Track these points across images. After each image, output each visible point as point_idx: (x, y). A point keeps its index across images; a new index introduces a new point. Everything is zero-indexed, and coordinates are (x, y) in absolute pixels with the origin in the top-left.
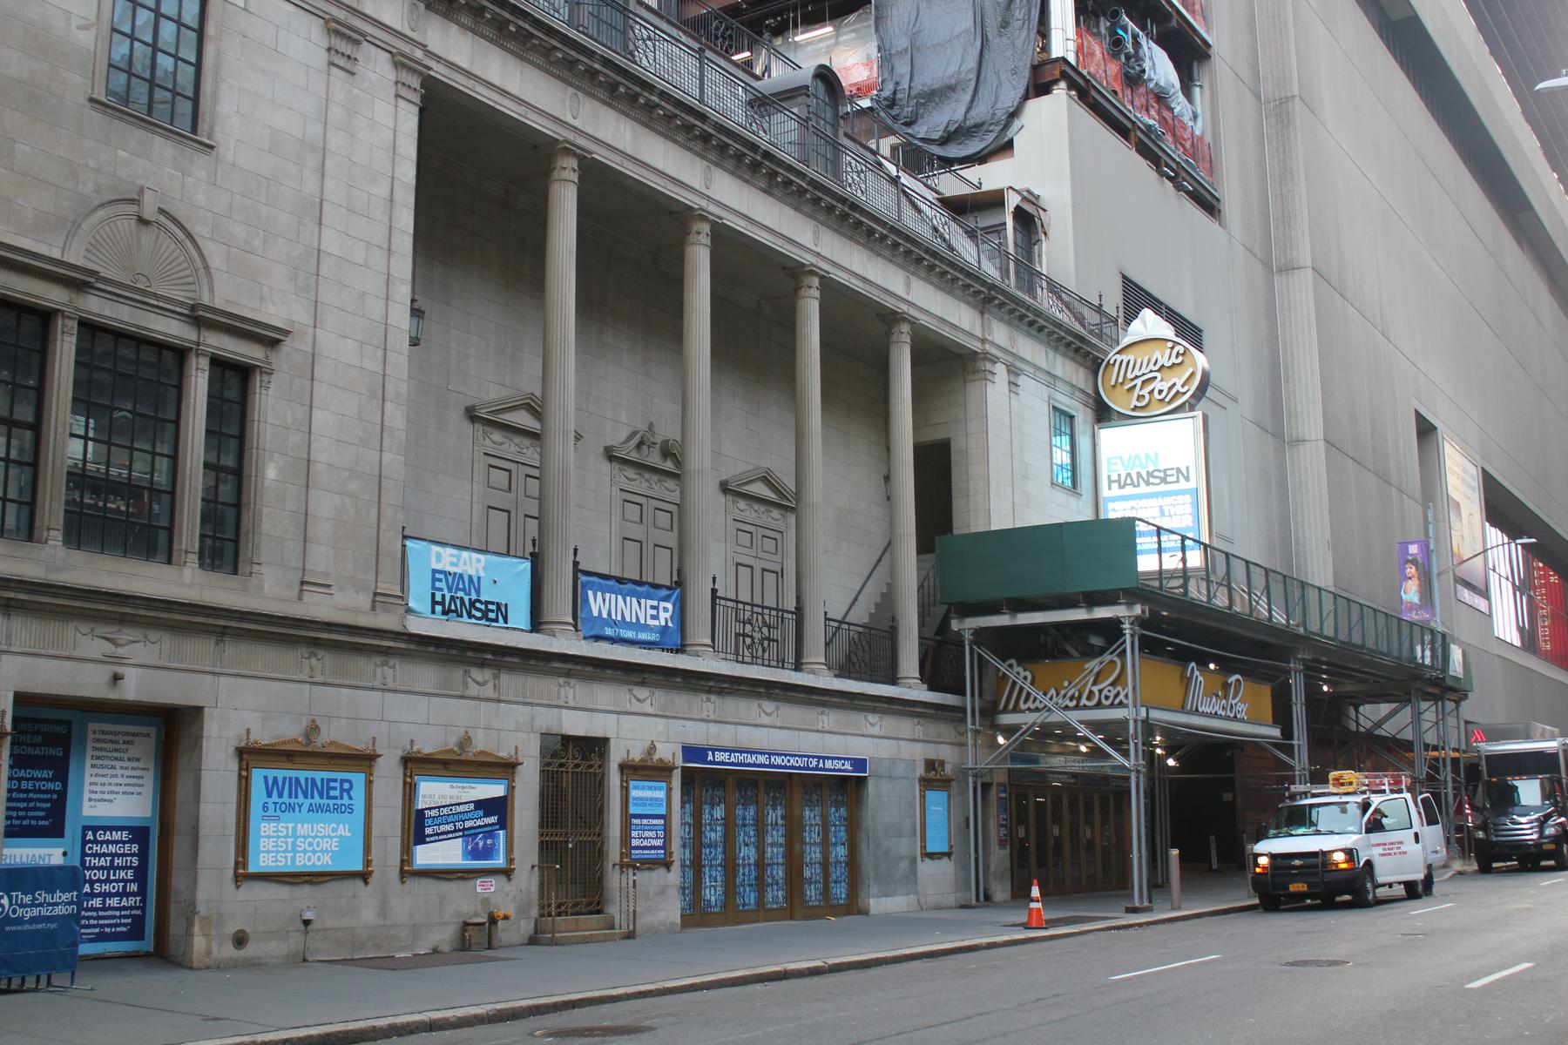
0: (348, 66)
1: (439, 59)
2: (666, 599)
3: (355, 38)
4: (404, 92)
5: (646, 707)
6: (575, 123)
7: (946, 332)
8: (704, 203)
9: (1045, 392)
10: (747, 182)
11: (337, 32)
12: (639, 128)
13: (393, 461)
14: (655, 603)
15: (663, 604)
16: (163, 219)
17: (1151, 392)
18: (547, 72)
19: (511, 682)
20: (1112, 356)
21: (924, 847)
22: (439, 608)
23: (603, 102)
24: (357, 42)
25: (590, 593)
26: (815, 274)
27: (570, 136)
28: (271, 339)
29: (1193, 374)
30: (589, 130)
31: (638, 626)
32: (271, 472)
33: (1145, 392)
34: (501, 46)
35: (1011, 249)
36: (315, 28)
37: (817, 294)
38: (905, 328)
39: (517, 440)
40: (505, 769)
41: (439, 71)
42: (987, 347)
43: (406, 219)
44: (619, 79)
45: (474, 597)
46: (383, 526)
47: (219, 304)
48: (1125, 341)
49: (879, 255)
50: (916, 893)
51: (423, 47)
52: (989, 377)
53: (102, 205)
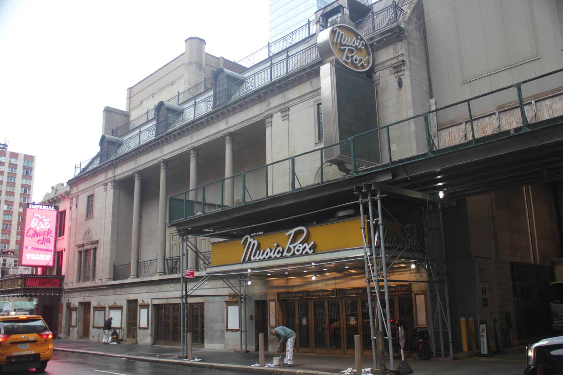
3: (107, 184)
5: (144, 291)
7: (246, 124)
10: (171, 142)
12: (147, 155)
19: (123, 290)
21: (227, 327)
28: (97, 242)
32: (97, 263)
36: (103, 187)
40: (120, 308)
41: (116, 178)
42: (266, 113)
50: (224, 343)
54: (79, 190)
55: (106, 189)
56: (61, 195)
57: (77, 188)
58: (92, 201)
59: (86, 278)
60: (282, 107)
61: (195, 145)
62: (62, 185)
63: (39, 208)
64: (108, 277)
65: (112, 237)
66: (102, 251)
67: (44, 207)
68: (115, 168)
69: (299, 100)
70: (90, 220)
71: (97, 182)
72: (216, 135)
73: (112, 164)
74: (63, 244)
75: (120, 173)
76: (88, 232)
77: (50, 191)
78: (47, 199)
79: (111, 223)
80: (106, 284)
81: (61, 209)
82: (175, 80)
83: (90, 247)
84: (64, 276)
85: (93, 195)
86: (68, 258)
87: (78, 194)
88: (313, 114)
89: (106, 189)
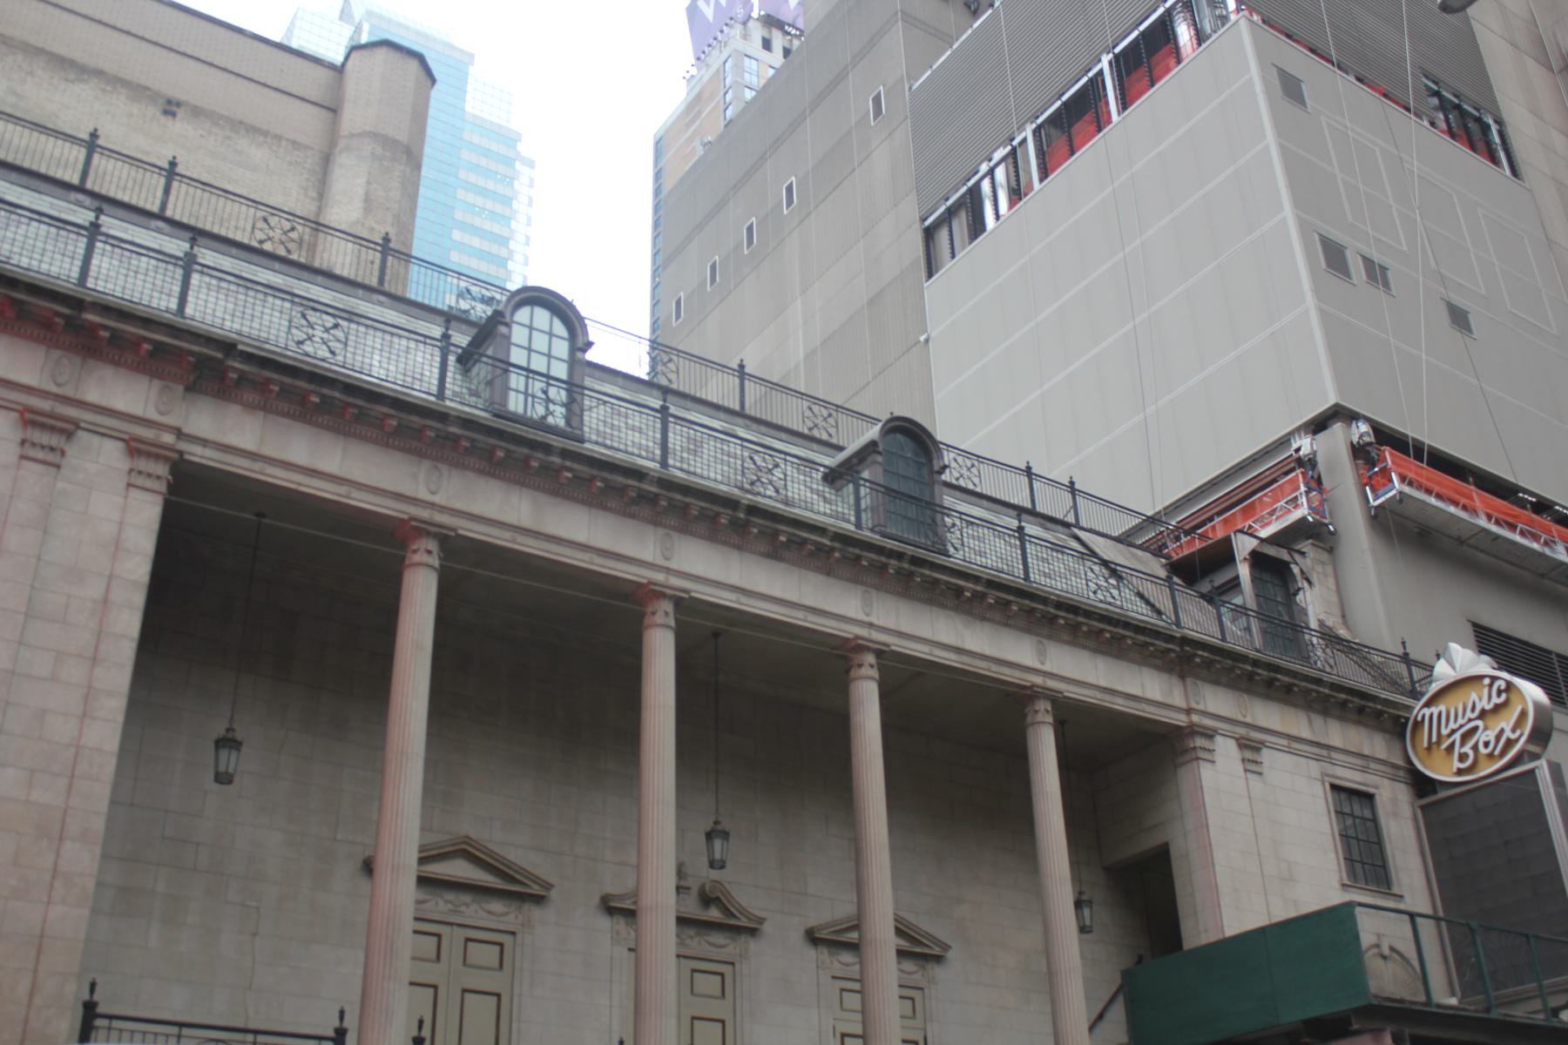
0: (51, 457)
1: (204, 442)
3: (68, 430)
4: (140, 481)
6: (436, 499)
7: (1119, 705)
8: (659, 577)
9: (1314, 768)
10: (739, 548)
11: (34, 424)
12: (543, 499)
13: (68, 918)
17: (1475, 748)
18: (387, 445)
20: (1419, 710)
23: (481, 472)
26: (868, 649)
27: (425, 514)
29: (1523, 714)
30: (459, 505)
33: (1467, 749)
34: (310, 423)
35: (1251, 603)
37: (875, 673)
38: (1043, 706)
39: (450, 896)
41: (198, 454)
42: (1195, 718)
43: (128, 622)
44: (492, 441)
46: (38, 1001)
48: (1435, 687)
49: (983, 619)
51: (179, 433)
52: (1202, 755)
60: (1242, 731)
61: (898, 645)
69: (1285, 742)
72: (994, 667)
73: (202, 363)
82: (197, 112)
88: (1323, 801)
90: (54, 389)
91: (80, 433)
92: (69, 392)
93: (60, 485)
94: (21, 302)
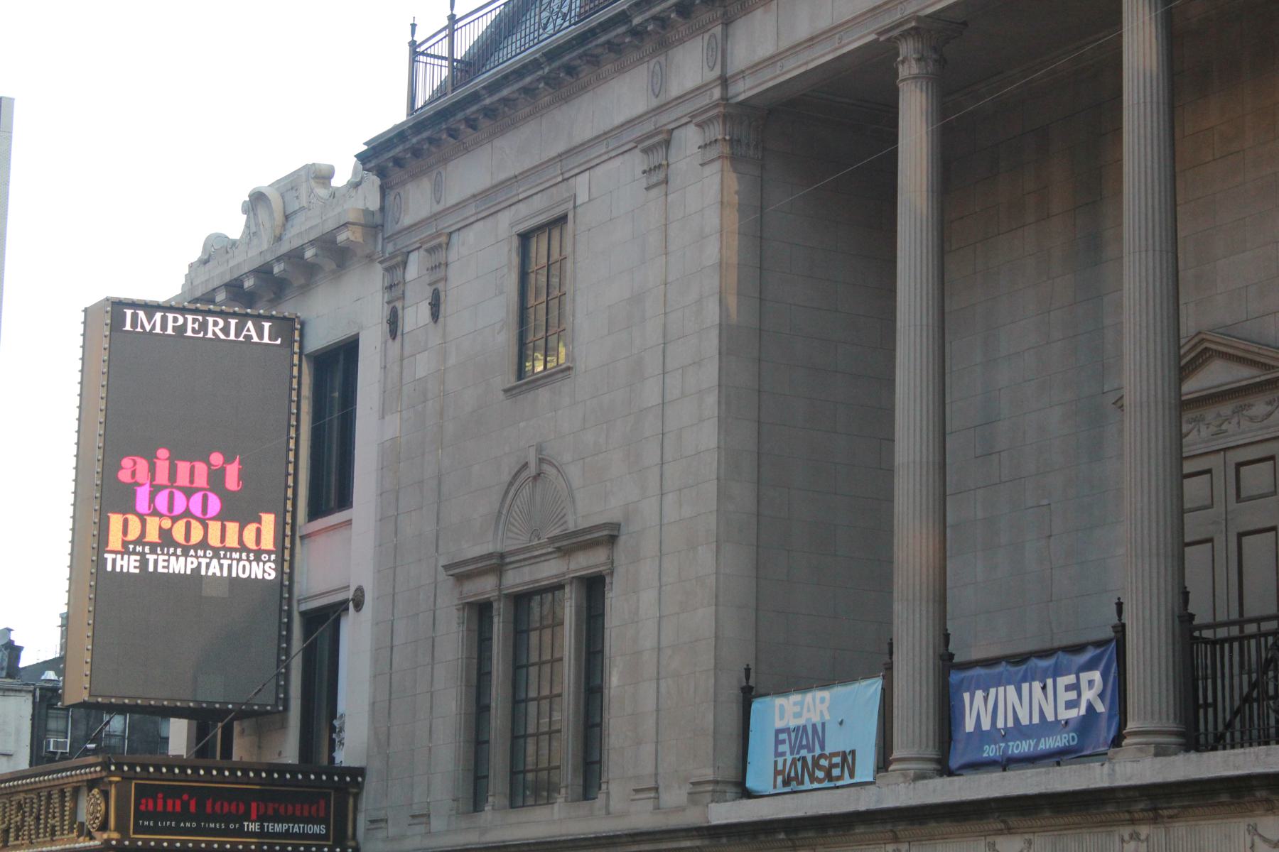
2: (1089, 666)
14: (1071, 679)
15: (1085, 677)
16: (545, 467)
22: (780, 779)
24: (667, 143)
25: (966, 696)
28: (609, 536)
31: (1045, 727)
36: (636, 162)
45: (818, 752)
47: (584, 524)
53: (511, 484)
54: (451, 199)
55: (658, 176)
56: (327, 243)
57: (437, 189)
58: (555, 266)
59: (528, 788)
62: (322, 175)
63: (181, 330)
64: (709, 774)
65: (722, 494)
66: (648, 597)
67: (214, 327)
68: (727, 24)
70: (543, 395)
71: (584, 132)
74: (343, 558)
75: (766, 49)
76: (534, 473)
77: (234, 226)
78: (220, 273)
79: (712, 400)
80: (692, 817)
81: (318, 340)
83: (549, 570)
84: (361, 771)
85: (560, 221)
86: (385, 651)
87: (449, 222)
89: (658, 176)
90: (655, 103)
91: (675, 133)
92: (663, 99)
93: (670, 198)
94: (608, 42)
